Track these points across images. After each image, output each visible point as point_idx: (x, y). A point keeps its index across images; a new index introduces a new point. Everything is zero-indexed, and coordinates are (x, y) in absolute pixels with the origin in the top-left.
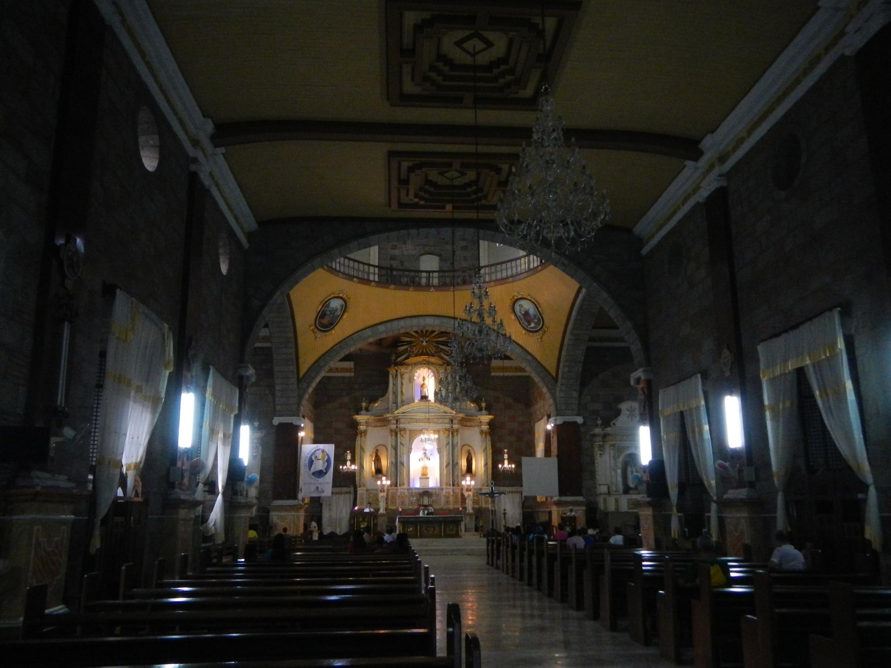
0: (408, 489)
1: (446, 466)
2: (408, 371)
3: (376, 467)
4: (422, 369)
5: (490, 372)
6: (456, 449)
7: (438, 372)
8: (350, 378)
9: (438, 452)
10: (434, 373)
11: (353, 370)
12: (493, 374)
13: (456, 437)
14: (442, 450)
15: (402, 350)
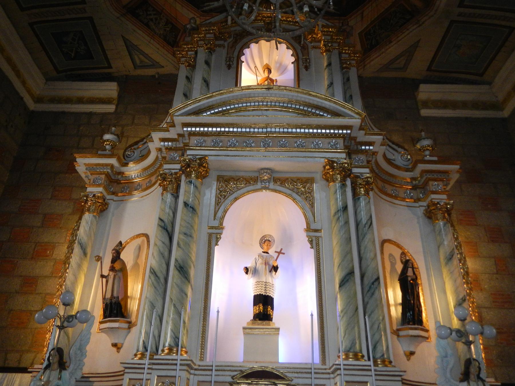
0: (189, 366)
1: (341, 286)
2: (226, 44)
3: (108, 296)
4: (263, 42)
5: (418, 111)
6: (368, 236)
7: (304, 48)
8: (104, 116)
9: (311, 242)
10: (294, 49)
11: (115, 102)
12: (425, 112)
13: (362, 203)
14: (322, 234)
15: (211, 7)
